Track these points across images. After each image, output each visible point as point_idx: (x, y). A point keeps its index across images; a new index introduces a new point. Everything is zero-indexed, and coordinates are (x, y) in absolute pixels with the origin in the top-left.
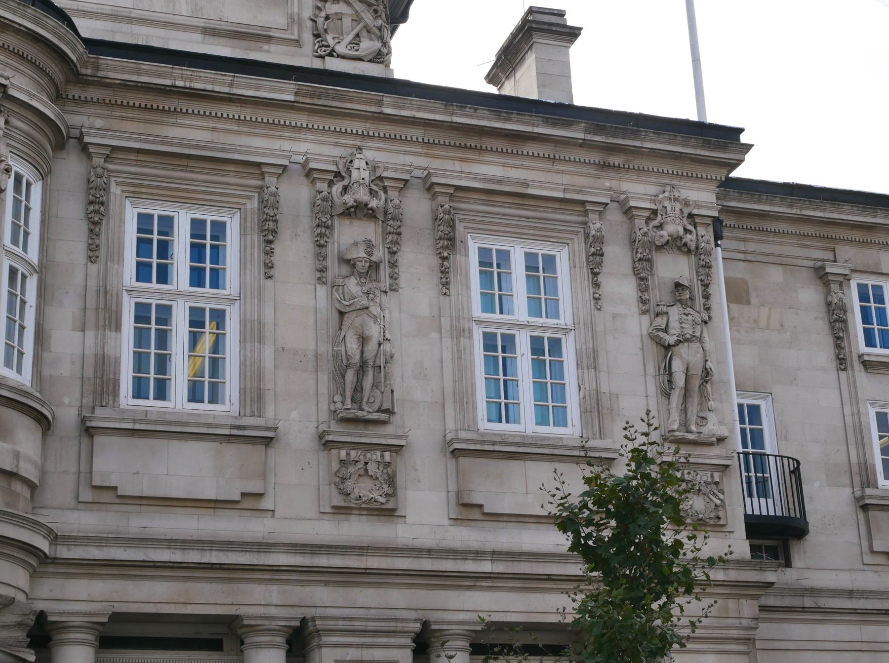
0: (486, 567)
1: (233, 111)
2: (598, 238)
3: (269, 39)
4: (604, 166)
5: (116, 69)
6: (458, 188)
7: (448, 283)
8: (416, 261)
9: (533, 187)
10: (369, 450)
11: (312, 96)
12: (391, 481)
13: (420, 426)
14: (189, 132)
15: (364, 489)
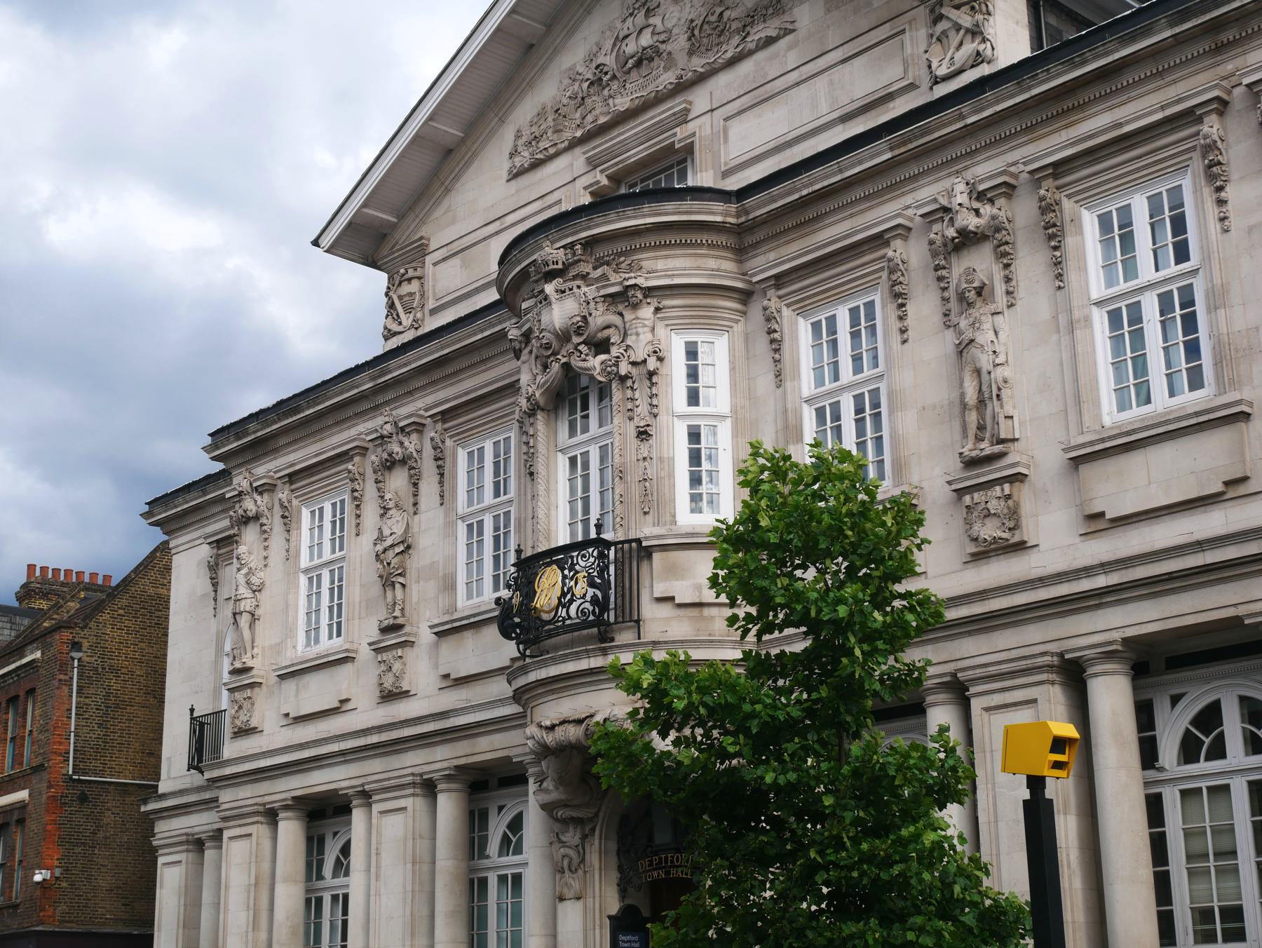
0: (1101, 581)
1: (859, 192)
2: (1209, 146)
3: (889, 97)
4: (1219, 49)
5: (761, 206)
6: (1055, 165)
7: (1061, 275)
8: (1030, 264)
9: (1128, 122)
10: (989, 488)
11: (904, 143)
12: (1014, 514)
13: (1038, 444)
14: (836, 231)
15: (989, 530)
